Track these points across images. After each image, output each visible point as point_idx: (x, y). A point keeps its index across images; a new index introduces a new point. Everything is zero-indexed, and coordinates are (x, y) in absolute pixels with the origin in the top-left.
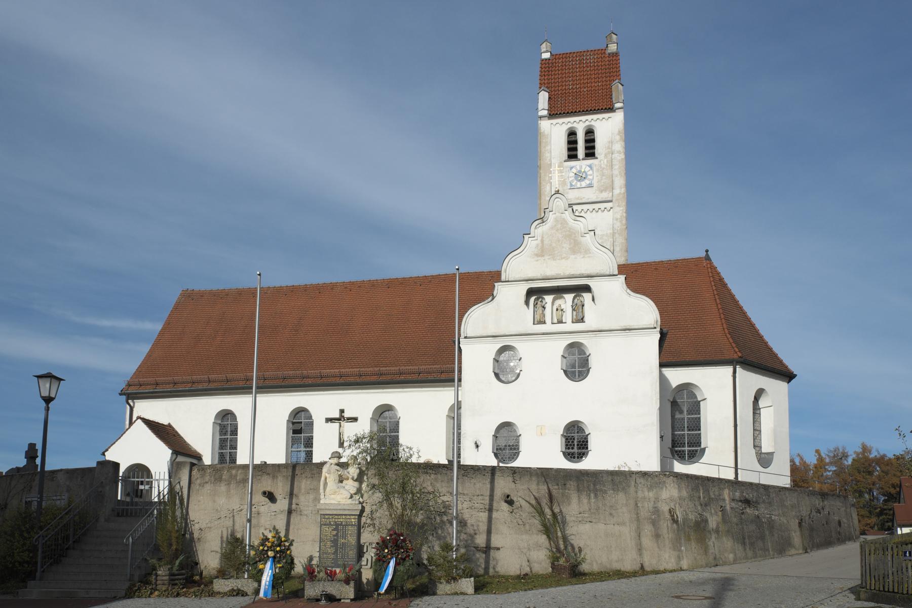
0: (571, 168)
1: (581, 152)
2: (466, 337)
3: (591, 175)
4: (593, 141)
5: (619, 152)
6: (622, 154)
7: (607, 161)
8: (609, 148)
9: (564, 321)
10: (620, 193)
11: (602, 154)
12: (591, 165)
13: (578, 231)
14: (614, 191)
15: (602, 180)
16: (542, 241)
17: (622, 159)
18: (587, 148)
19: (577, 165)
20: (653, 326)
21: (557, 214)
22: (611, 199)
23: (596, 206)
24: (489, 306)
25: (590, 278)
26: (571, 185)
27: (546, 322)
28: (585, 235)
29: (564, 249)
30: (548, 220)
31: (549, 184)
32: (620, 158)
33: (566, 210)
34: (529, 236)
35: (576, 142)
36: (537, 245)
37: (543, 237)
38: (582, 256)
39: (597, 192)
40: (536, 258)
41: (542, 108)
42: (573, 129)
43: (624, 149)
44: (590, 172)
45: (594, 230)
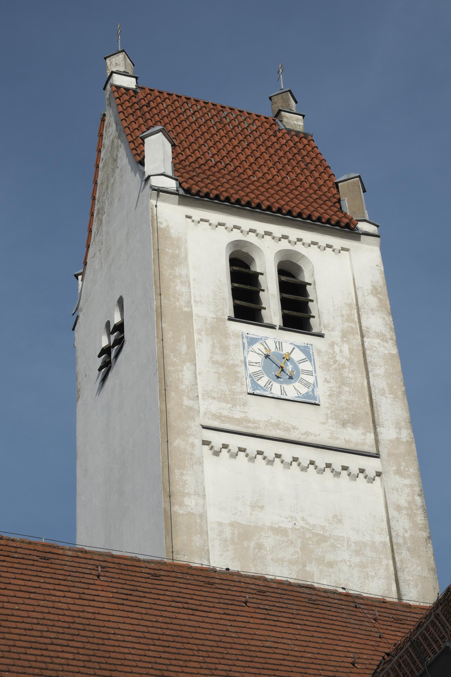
0: (252, 341)
3: (309, 373)
6: (390, 342)
7: (351, 351)
10: (397, 439)
11: (333, 330)
12: (307, 347)
14: (378, 429)
15: (340, 393)
17: (392, 355)
19: (266, 338)
26: (255, 385)
31: (188, 364)
39: (330, 420)
42: (245, 250)
43: (393, 334)
44: (306, 366)
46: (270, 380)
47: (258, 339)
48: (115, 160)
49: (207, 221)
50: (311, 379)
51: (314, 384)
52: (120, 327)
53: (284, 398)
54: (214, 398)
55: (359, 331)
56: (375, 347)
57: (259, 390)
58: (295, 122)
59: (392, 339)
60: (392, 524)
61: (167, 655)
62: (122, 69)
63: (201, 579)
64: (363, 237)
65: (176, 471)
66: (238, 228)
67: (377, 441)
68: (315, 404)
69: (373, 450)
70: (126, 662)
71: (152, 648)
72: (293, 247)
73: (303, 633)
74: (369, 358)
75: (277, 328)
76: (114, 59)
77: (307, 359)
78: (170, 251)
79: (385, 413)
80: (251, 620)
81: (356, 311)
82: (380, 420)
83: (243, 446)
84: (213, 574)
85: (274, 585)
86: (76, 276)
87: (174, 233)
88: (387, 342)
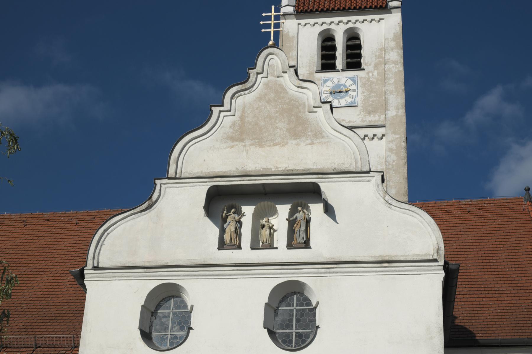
0: (326, 81)
1: (340, 62)
3: (354, 91)
4: (359, 47)
5: (395, 62)
8: (380, 57)
9: (275, 246)
10: (396, 115)
11: (370, 65)
13: (305, 103)
15: (370, 97)
16: (242, 117)
17: (400, 71)
18: (348, 56)
19: (333, 78)
20: (431, 258)
21: (270, 78)
22: (383, 123)
24: (141, 217)
25: (320, 176)
27: (242, 245)
28: (315, 110)
29: (278, 130)
30: (255, 87)
32: (397, 70)
33: (285, 72)
34: (221, 109)
35: (334, 48)
36: (234, 124)
37: (243, 112)
38: (308, 142)
40: (230, 143)
41: (286, 4)
42: (331, 33)
45: (330, 102)
46: (333, 99)
47: (329, 79)
49: (309, 24)
50: (354, 94)
51: (356, 96)
56: (390, 69)
59: (400, 63)
60: (387, 159)
64: (392, 10)
66: (325, 23)
68: (355, 106)
72: (354, 25)
74: (387, 76)
75: (341, 71)
77: (354, 84)
78: (288, 45)
79: (391, 103)
82: (388, 107)
87: (291, 34)
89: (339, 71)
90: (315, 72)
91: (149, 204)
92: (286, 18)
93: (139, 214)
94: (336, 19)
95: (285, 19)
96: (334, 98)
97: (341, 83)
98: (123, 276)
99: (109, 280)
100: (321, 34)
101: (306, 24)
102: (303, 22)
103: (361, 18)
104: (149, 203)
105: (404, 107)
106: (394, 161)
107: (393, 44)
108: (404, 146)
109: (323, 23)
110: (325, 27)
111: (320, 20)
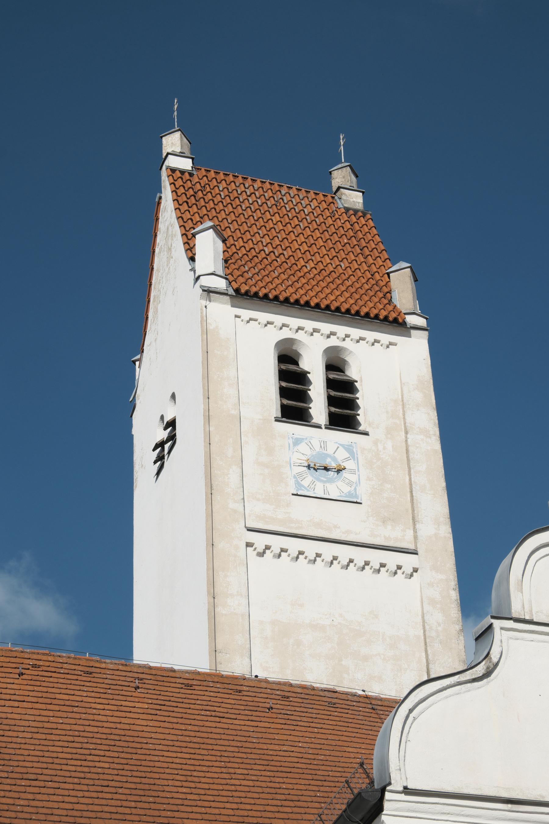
0: (297, 442)
2: (407, 791)
12: (351, 446)
14: (417, 526)
18: (331, 401)
23: (376, 557)
26: (299, 485)
42: (294, 348)
46: (314, 480)
47: (303, 439)
48: (170, 249)
49: (256, 320)
50: (353, 478)
51: (356, 483)
52: (172, 424)
53: (327, 498)
54: (258, 500)
55: (403, 427)
57: (303, 490)
58: (354, 200)
59: (435, 435)
61: (192, 762)
62: (178, 150)
63: (230, 687)
65: (220, 573)
66: (287, 326)
67: (416, 538)
68: (357, 503)
69: (411, 547)
70: (155, 770)
71: (179, 755)
72: (341, 343)
73: (319, 736)
74: (412, 455)
75: (323, 427)
76: (170, 139)
77: (351, 458)
79: (424, 510)
80: (273, 726)
81: (401, 407)
82: (419, 517)
83: (285, 547)
84: (242, 682)
85: (299, 690)
86: (134, 362)
88: (430, 438)
89: (319, 427)
90: (274, 419)
91: (488, 668)
92: (212, 299)
93: (469, 685)
94: (309, 324)
95: (210, 301)
96: (315, 478)
97: (325, 452)
98: (463, 813)
99: (434, 820)
100: (279, 344)
101: (251, 319)
102: (246, 314)
103: (356, 332)
104: (487, 664)
105: (448, 521)
106: (439, 625)
107: (418, 396)
108: (455, 598)
109: (284, 325)
110: (286, 334)
111: (279, 319)
